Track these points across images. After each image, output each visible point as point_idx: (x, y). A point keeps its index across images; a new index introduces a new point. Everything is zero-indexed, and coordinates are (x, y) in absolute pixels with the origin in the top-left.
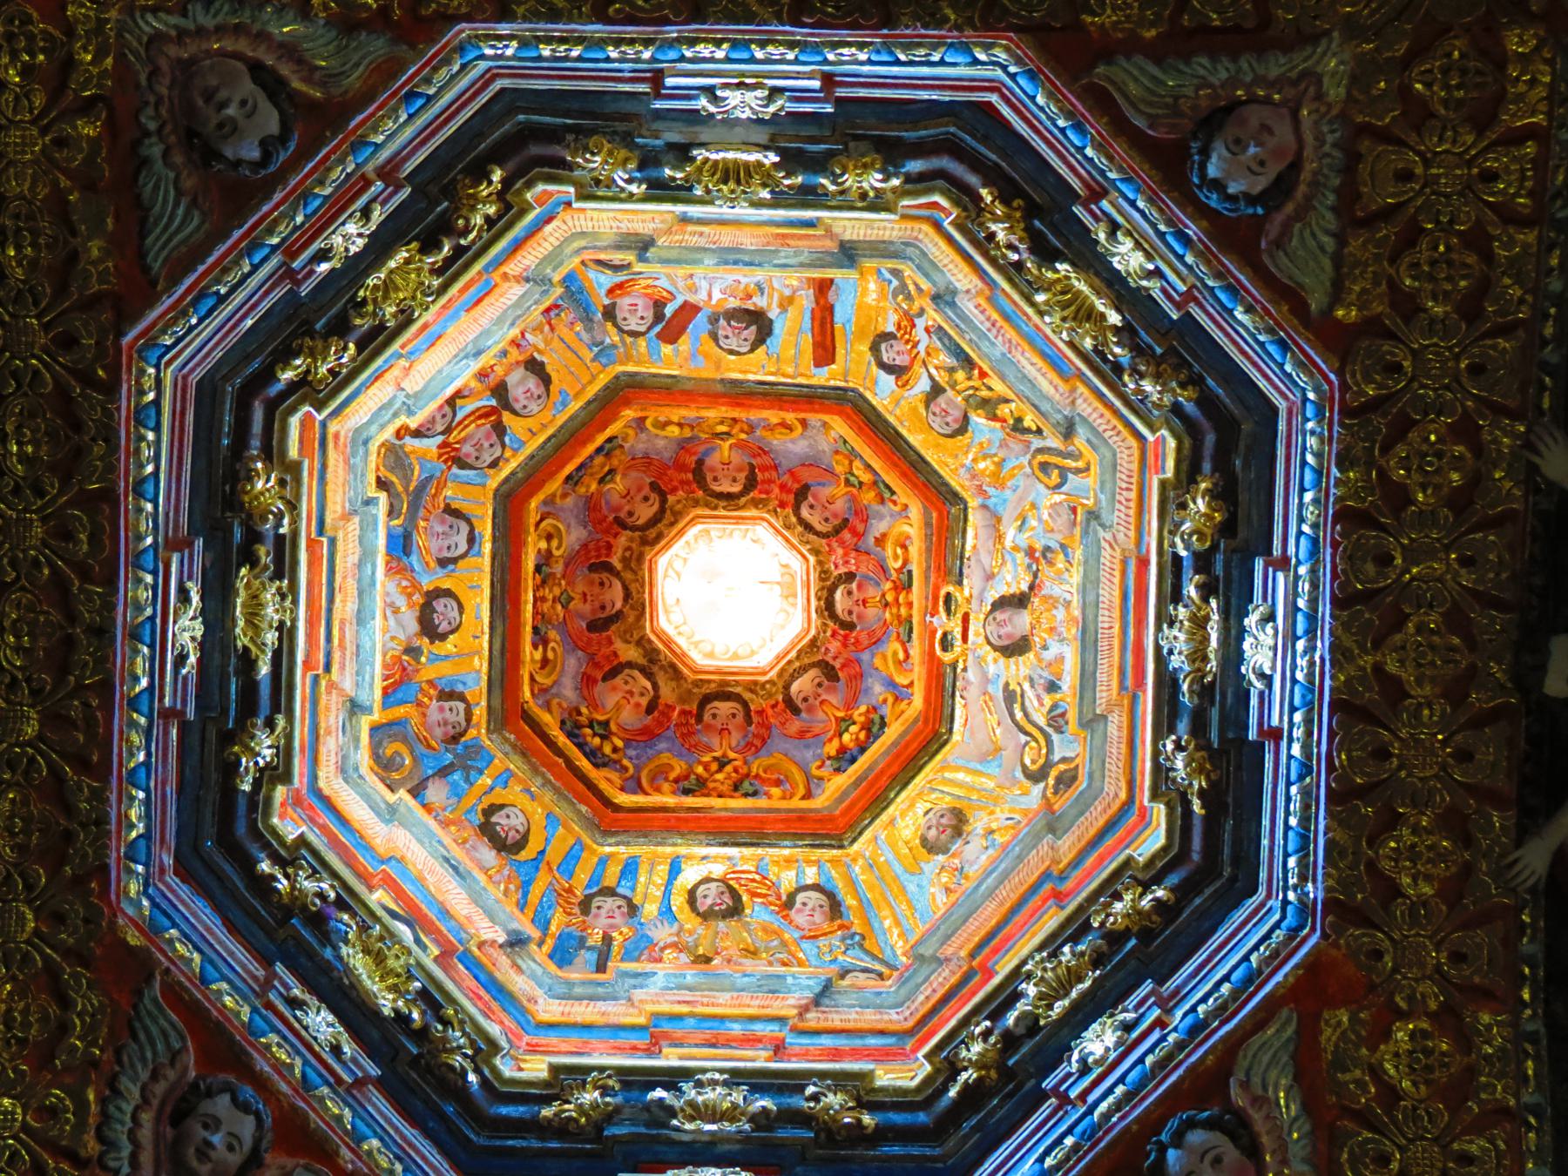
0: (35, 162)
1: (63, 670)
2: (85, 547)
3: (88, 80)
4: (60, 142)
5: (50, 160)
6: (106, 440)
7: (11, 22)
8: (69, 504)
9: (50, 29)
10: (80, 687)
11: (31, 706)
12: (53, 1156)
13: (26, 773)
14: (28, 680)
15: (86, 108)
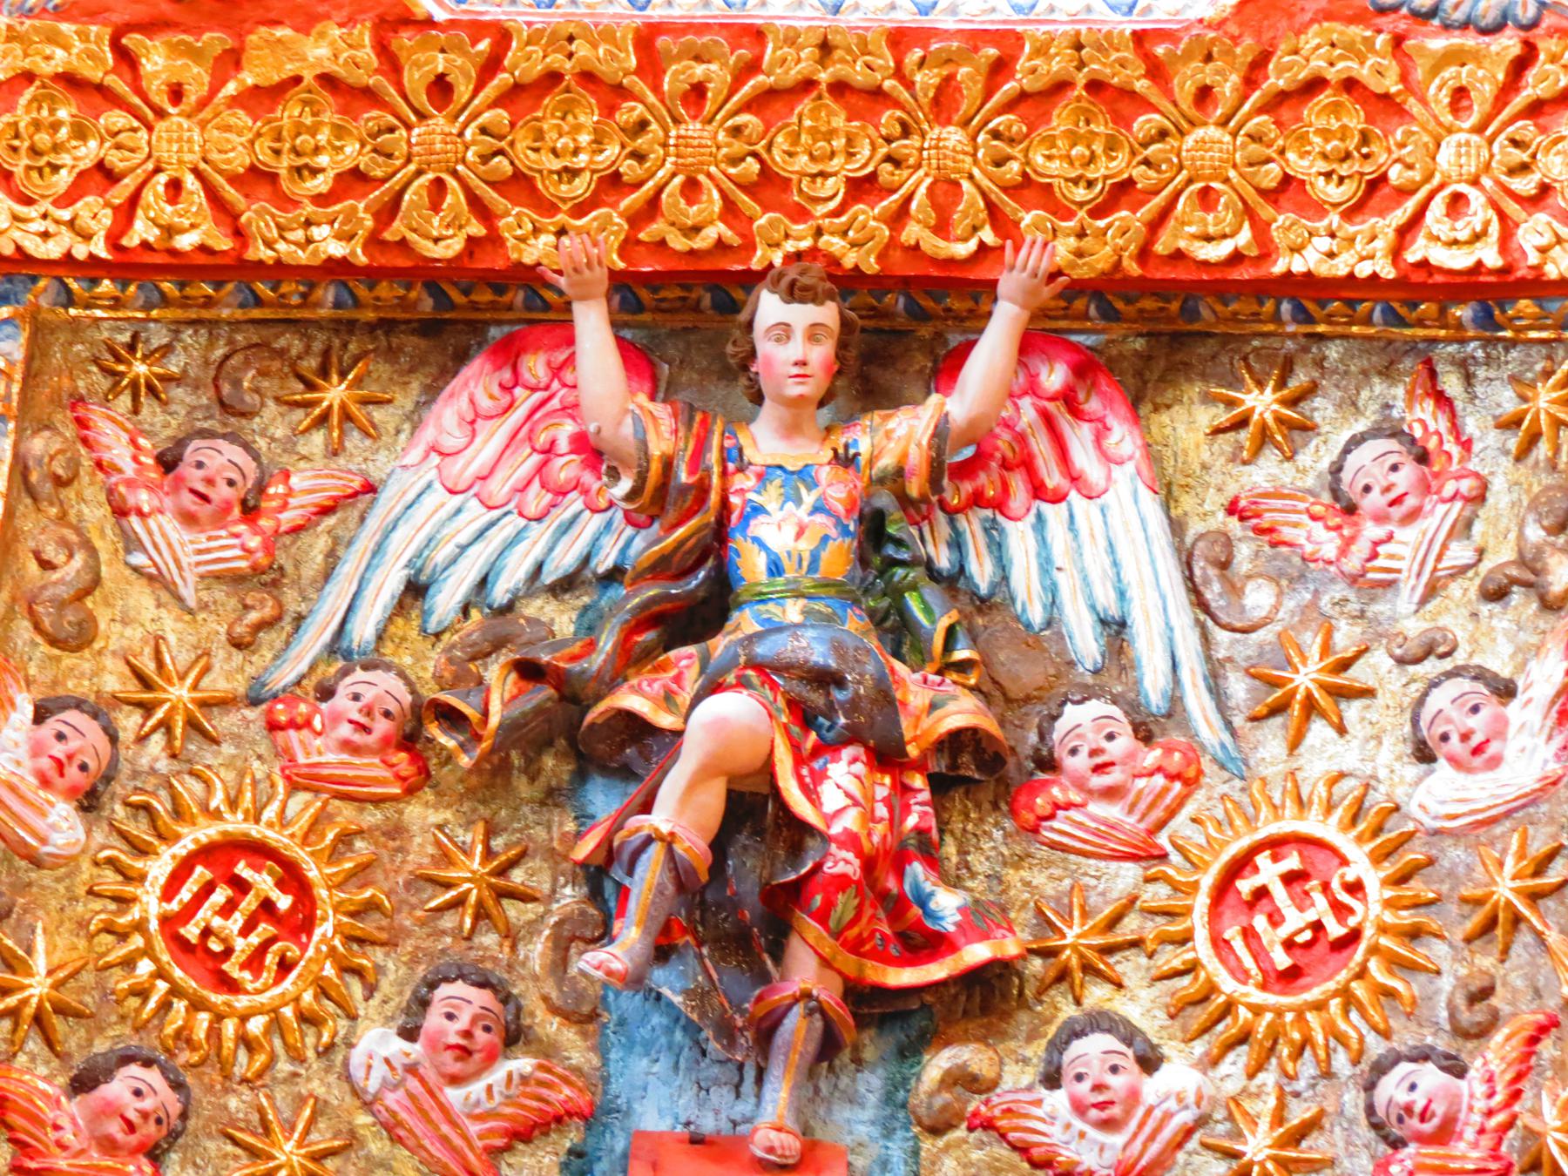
0: (203, 125)
1: (877, 95)
2: (714, 67)
3: (91, 55)
4: (176, 94)
5: (203, 103)
6: (571, 39)
7: (15, 149)
8: (656, 88)
9: (22, 102)
10: (899, 73)
11: (923, 135)
12: (1517, 90)
13: (1012, 141)
14: (888, 140)
15: (127, 59)
